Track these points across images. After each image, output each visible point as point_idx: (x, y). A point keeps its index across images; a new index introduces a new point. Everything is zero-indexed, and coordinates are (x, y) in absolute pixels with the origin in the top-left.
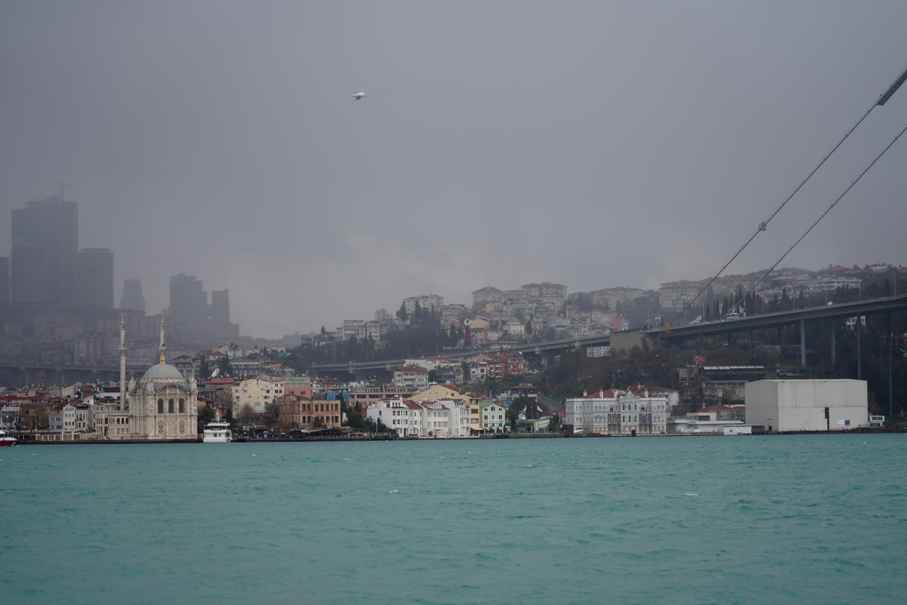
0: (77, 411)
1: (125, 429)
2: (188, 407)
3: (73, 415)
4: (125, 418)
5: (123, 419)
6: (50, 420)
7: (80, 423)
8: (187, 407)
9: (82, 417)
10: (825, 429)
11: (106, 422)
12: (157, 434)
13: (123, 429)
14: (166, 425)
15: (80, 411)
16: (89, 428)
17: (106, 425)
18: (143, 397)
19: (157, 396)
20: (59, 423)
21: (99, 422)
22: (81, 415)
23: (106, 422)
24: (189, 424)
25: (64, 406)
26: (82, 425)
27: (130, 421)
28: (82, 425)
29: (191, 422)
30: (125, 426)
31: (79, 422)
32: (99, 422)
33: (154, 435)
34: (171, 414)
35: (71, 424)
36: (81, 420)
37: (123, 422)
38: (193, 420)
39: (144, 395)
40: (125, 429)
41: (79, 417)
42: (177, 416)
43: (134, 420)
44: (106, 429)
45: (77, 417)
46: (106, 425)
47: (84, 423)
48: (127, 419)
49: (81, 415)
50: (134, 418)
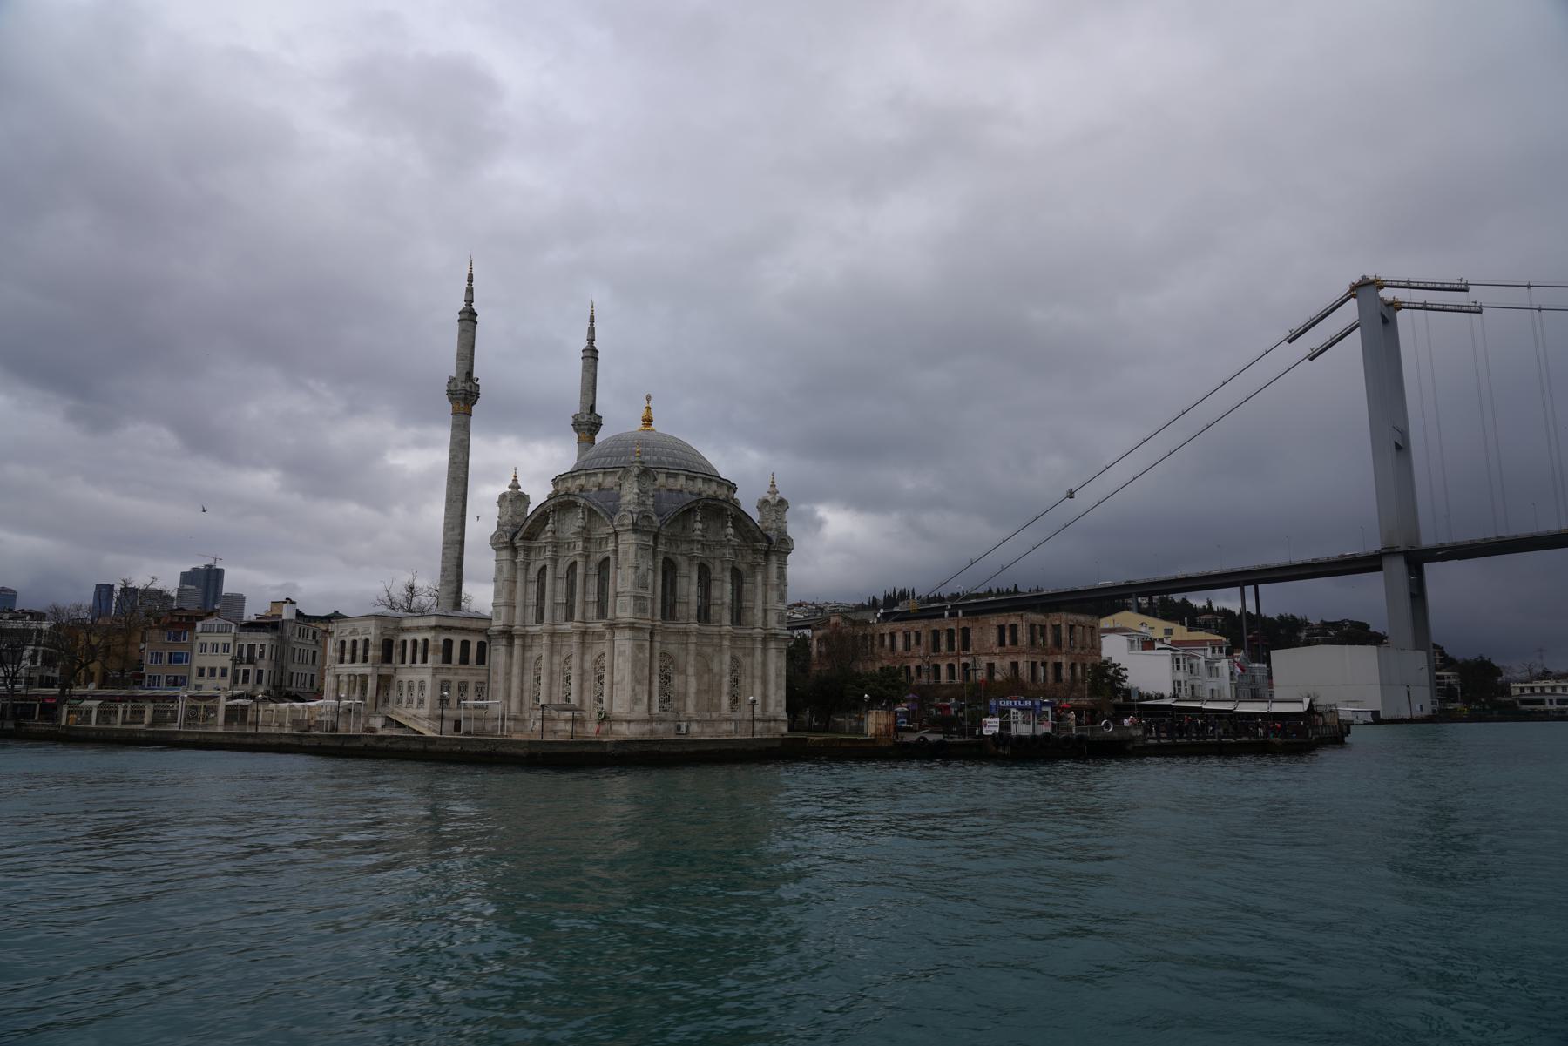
0: (243, 635)
1: (471, 687)
2: (759, 602)
3: (226, 647)
4: (474, 641)
5: (465, 645)
6: (147, 659)
7: (246, 672)
8: (754, 601)
9: (257, 655)
10: (1407, 715)
11: (387, 657)
12: (656, 710)
13: (463, 687)
14: (684, 672)
15: (253, 635)
16: (274, 687)
17: (386, 669)
18: (585, 548)
19: (662, 540)
20: (177, 670)
21: (347, 657)
22: (252, 647)
23: (387, 657)
24: (758, 673)
25: (201, 619)
26: (252, 677)
27: (498, 654)
28: (252, 677)
29: (765, 664)
30: (472, 675)
31: (242, 668)
32: (347, 657)
33: (647, 716)
34: (463, 666)
35: (218, 673)
36: (251, 660)
37: (464, 659)
38: (772, 654)
39: (587, 540)
40: (471, 687)
41: (245, 655)
42: (721, 636)
43: (517, 651)
44: (385, 682)
45: (240, 653)
46: (386, 669)
47: (260, 672)
48: (482, 646)
49: (252, 647)
50: (517, 642)
